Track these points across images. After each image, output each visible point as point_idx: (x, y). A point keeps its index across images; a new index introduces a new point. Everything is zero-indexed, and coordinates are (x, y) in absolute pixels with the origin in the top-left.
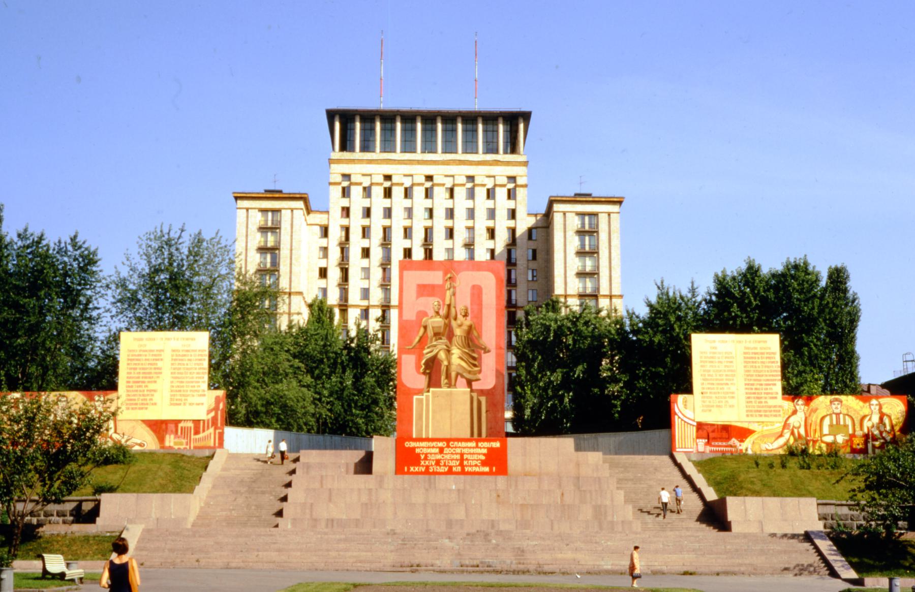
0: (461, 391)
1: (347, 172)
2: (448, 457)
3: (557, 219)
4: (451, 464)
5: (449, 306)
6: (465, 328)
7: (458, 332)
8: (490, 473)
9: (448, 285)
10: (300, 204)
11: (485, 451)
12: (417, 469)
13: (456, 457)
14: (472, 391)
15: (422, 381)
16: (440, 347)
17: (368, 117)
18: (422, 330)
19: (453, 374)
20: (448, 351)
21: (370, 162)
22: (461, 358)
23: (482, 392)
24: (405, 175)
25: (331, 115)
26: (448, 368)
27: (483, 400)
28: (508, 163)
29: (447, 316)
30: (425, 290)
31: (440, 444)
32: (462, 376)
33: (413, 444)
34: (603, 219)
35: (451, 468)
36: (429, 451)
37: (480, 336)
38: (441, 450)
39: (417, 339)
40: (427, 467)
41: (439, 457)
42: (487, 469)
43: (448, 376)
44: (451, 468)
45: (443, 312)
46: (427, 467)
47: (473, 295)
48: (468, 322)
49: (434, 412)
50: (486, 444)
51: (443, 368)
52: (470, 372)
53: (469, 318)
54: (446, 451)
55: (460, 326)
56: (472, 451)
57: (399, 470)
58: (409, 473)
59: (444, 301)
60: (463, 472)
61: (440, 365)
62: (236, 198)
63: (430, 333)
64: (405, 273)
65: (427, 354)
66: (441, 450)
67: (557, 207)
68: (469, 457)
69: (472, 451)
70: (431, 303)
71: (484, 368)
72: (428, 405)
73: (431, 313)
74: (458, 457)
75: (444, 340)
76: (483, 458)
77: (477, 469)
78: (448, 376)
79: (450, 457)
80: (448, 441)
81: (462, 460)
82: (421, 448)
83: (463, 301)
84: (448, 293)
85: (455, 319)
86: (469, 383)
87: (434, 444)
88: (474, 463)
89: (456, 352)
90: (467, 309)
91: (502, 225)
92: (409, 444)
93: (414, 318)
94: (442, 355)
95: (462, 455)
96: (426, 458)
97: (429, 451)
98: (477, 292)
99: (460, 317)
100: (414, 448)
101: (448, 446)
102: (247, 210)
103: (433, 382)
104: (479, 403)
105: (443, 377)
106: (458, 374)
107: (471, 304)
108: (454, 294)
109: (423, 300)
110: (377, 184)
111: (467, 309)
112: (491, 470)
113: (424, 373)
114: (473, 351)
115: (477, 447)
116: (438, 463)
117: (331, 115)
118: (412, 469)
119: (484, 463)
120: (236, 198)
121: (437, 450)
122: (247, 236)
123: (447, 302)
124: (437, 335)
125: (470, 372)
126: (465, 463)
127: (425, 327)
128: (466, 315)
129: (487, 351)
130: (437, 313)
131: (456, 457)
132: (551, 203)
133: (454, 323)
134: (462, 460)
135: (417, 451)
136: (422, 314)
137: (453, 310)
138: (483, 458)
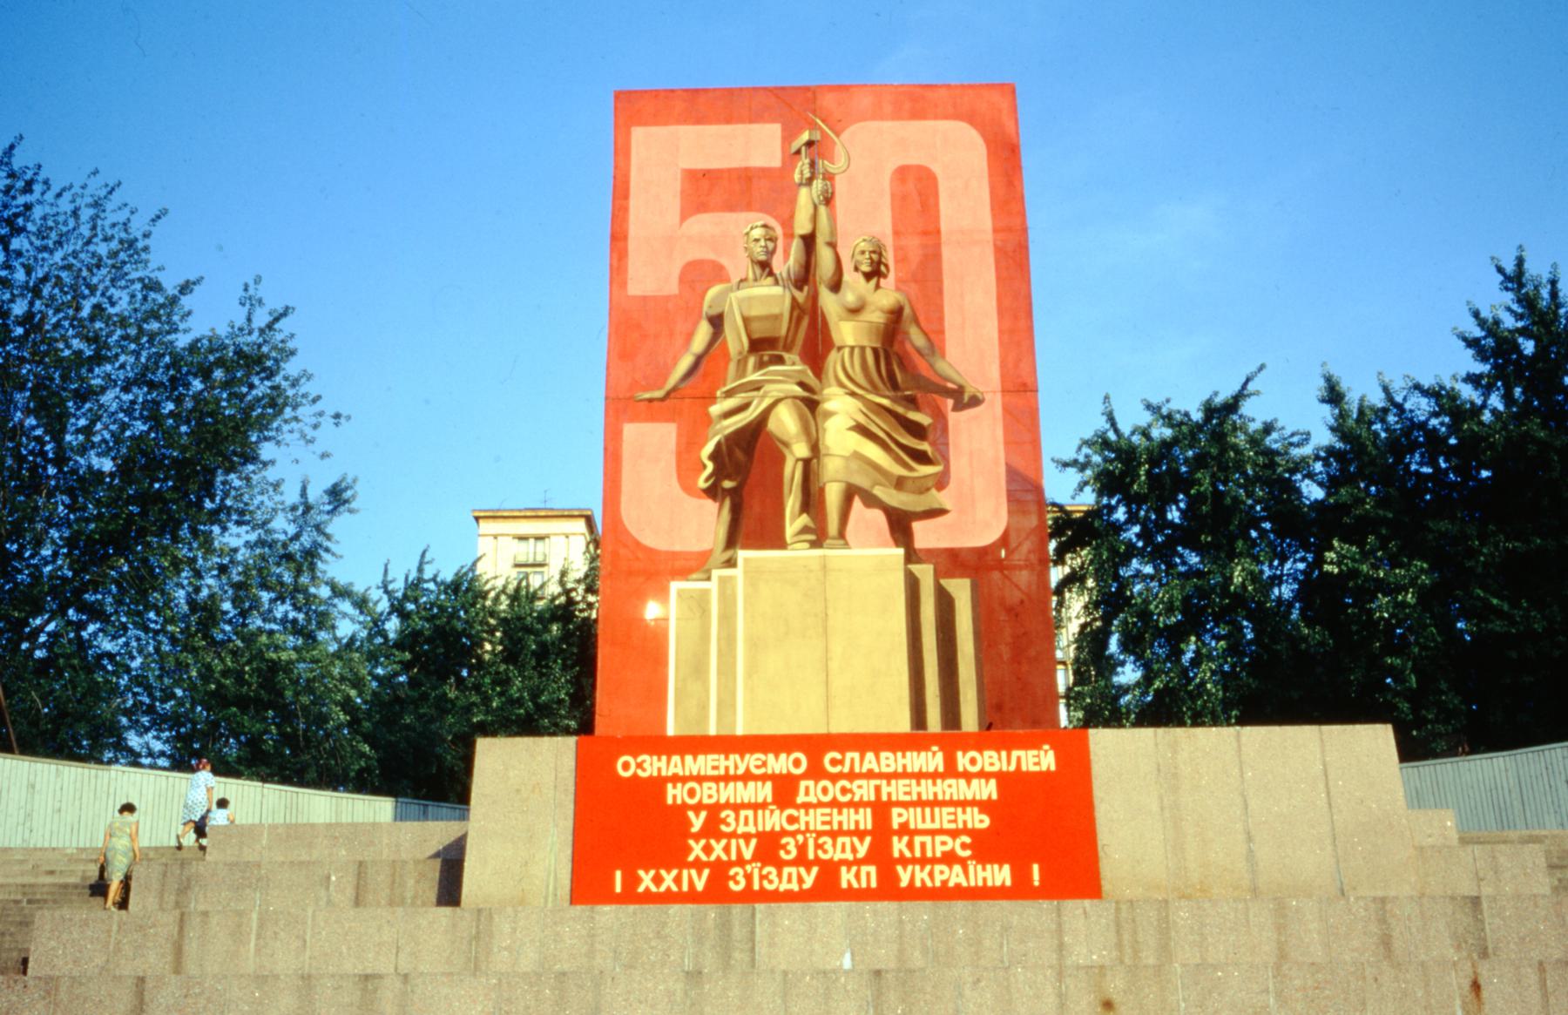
0: (869, 564)
2: (816, 819)
4: (833, 852)
5: (809, 241)
6: (876, 317)
7: (847, 333)
8: (1020, 890)
9: (802, 168)
11: (989, 790)
12: (669, 879)
13: (849, 819)
14: (912, 556)
15: (705, 523)
16: (774, 391)
18: (703, 332)
19: (833, 495)
20: (811, 405)
22: (861, 430)
23: (953, 561)
26: (809, 468)
27: (961, 590)
29: (805, 277)
30: (706, 190)
31: (780, 764)
32: (871, 501)
33: (652, 765)
35: (829, 871)
36: (728, 793)
37: (936, 345)
38: (785, 791)
39: (685, 363)
40: (720, 872)
41: (774, 820)
42: (1000, 875)
43: (811, 501)
44: (829, 871)
45: (787, 262)
46: (720, 872)
47: (900, 202)
48: (886, 297)
49: (754, 644)
50: (992, 760)
51: (792, 472)
52: (900, 483)
53: (889, 282)
54: (809, 791)
55: (855, 311)
56: (927, 790)
57: (588, 885)
58: (631, 895)
59: (788, 223)
60: (888, 889)
61: (779, 460)
62: (477, 519)
63: (736, 339)
64: (638, 134)
65: (724, 419)
66: (785, 791)
68: (914, 817)
69: (927, 790)
70: (745, 229)
71: (959, 465)
72: (727, 618)
73: (739, 266)
74: (865, 819)
75: (794, 365)
76: (981, 821)
77: (955, 876)
78: (811, 501)
79: (828, 819)
80: (814, 745)
81: (882, 832)
82: (689, 781)
83: (863, 219)
84: (805, 199)
85: (836, 286)
86: (900, 526)
87: (752, 761)
88: (942, 845)
89: (842, 408)
90: (878, 251)
92: (629, 766)
93: (672, 287)
94: (786, 422)
95: (881, 809)
96: (712, 829)
97: (728, 793)
98: (917, 191)
99: (849, 276)
100: (659, 783)
101: (816, 772)
103: (751, 523)
104: (945, 604)
105: (792, 502)
106: (850, 493)
107: (896, 233)
108: (828, 200)
109: (704, 224)
111: (878, 251)
112: (1021, 876)
113: (712, 492)
114: (912, 402)
115: (951, 771)
116: (768, 847)
118: (646, 880)
119: (985, 848)
120: (477, 519)
121: (765, 791)
123: (802, 226)
124: (763, 347)
125: (900, 483)
126: (898, 846)
127: (717, 322)
128: (875, 273)
129: (965, 400)
130: (765, 266)
131: (849, 819)
133: (830, 303)
134: (882, 832)
135: (675, 794)
136: (701, 274)
137: (824, 256)
138: (981, 821)
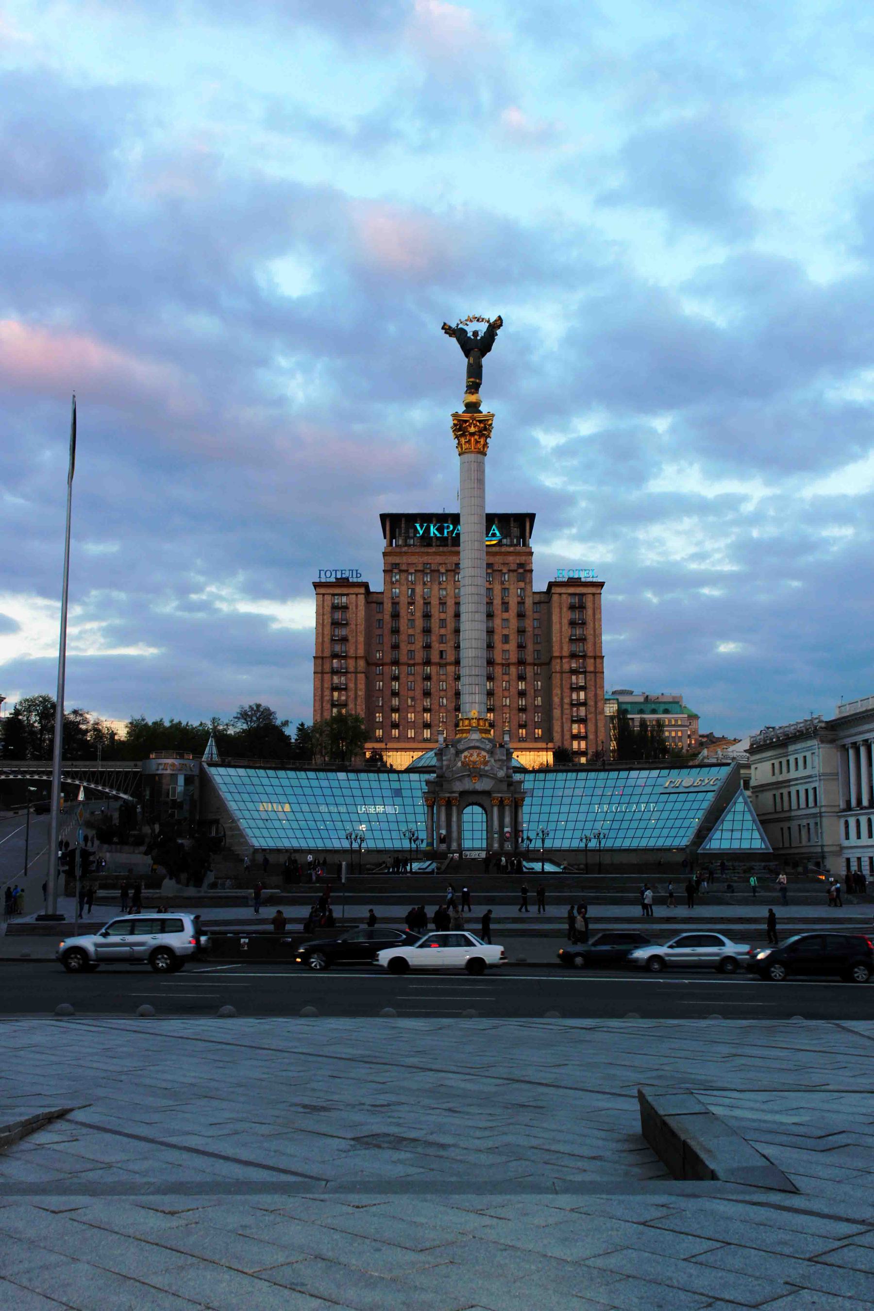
1: (397, 562)
3: (555, 598)
10: (362, 590)
17: (411, 519)
21: (413, 554)
24: (441, 564)
25: (384, 517)
28: (519, 554)
34: (590, 598)
67: (555, 590)
91: (513, 602)
102: (324, 595)
110: (420, 571)
117: (384, 517)
122: (323, 614)
132: (551, 585)
